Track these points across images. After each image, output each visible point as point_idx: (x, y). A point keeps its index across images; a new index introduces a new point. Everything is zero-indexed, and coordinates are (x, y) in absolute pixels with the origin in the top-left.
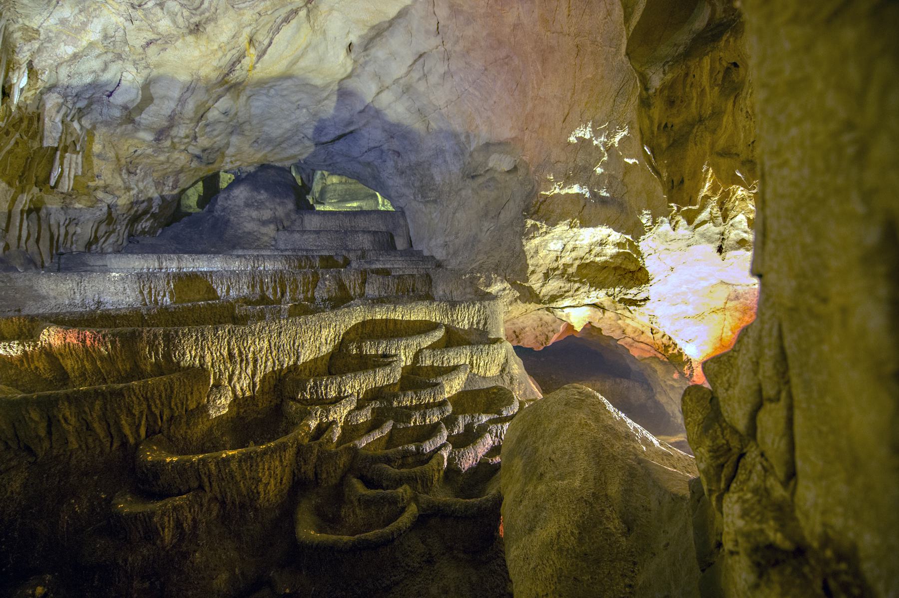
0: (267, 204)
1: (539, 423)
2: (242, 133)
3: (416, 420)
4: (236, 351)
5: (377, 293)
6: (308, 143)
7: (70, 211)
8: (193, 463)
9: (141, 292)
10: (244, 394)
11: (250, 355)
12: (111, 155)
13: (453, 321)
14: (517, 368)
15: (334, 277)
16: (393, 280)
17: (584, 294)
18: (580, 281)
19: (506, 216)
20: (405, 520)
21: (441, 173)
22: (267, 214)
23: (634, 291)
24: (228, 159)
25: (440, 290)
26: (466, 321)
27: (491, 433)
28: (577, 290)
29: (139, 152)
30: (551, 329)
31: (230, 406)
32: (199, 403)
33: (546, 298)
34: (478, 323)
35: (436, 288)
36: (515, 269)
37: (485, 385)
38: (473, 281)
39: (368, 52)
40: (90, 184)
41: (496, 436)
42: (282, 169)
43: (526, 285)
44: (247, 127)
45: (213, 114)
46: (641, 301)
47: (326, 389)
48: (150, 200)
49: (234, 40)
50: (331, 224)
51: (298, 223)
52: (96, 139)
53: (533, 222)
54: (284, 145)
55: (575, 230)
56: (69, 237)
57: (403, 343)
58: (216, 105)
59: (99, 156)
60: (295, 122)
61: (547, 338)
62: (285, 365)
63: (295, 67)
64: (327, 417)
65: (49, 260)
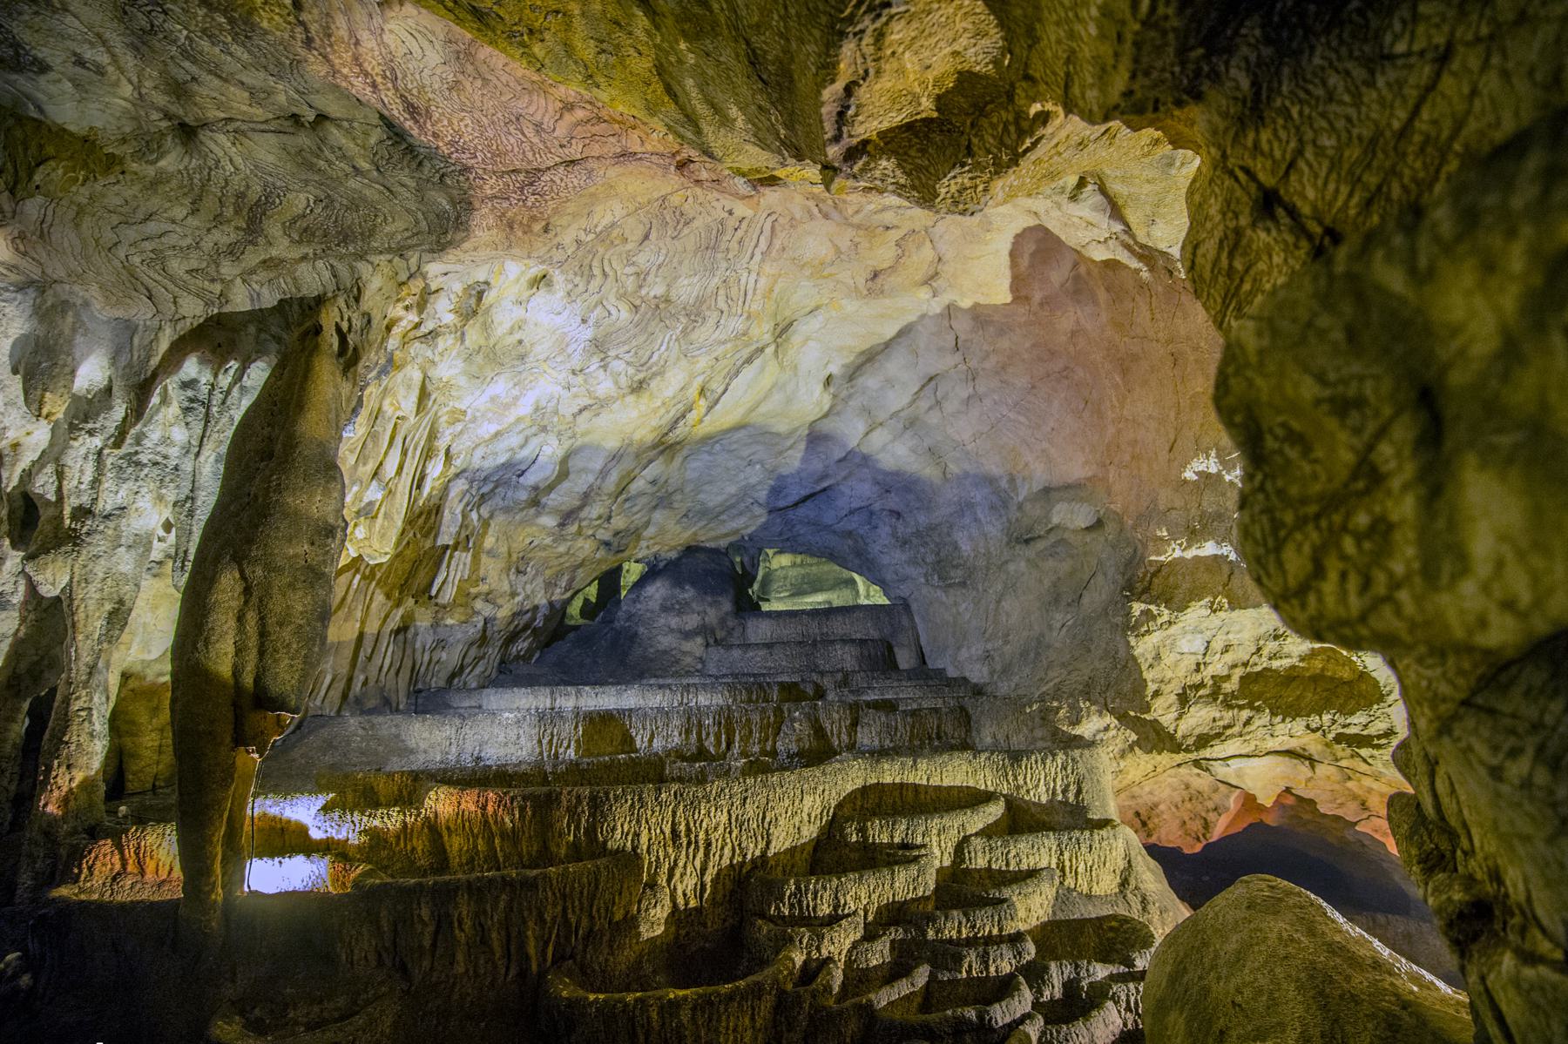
0: (694, 605)
1: (1205, 944)
2: (670, 506)
4: (682, 828)
5: (877, 743)
6: (758, 510)
10: (687, 904)
11: (702, 836)
13: (1018, 788)
14: (1151, 878)
15: (808, 716)
16: (903, 719)
17: (1262, 731)
18: (1251, 706)
19: (1094, 598)
21: (971, 538)
22: (692, 621)
23: (1359, 718)
24: (643, 544)
25: (986, 736)
26: (1042, 788)
28: (1248, 722)
30: (1210, 805)
33: (1190, 741)
34: (1064, 791)
35: (979, 732)
36: (1123, 691)
37: (1093, 912)
38: (1046, 716)
41: (1128, 1009)
42: (715, 551)
43: (1147, 717)
46: (1379, 737)
47: (815, 899)
50: (790, 631)
53: (1143, 606)
54: (723, 517)
55: (1222, 614)
57: (935, 823)
61: (1207, 825)
62: (749, 857)
64: (818, 949)
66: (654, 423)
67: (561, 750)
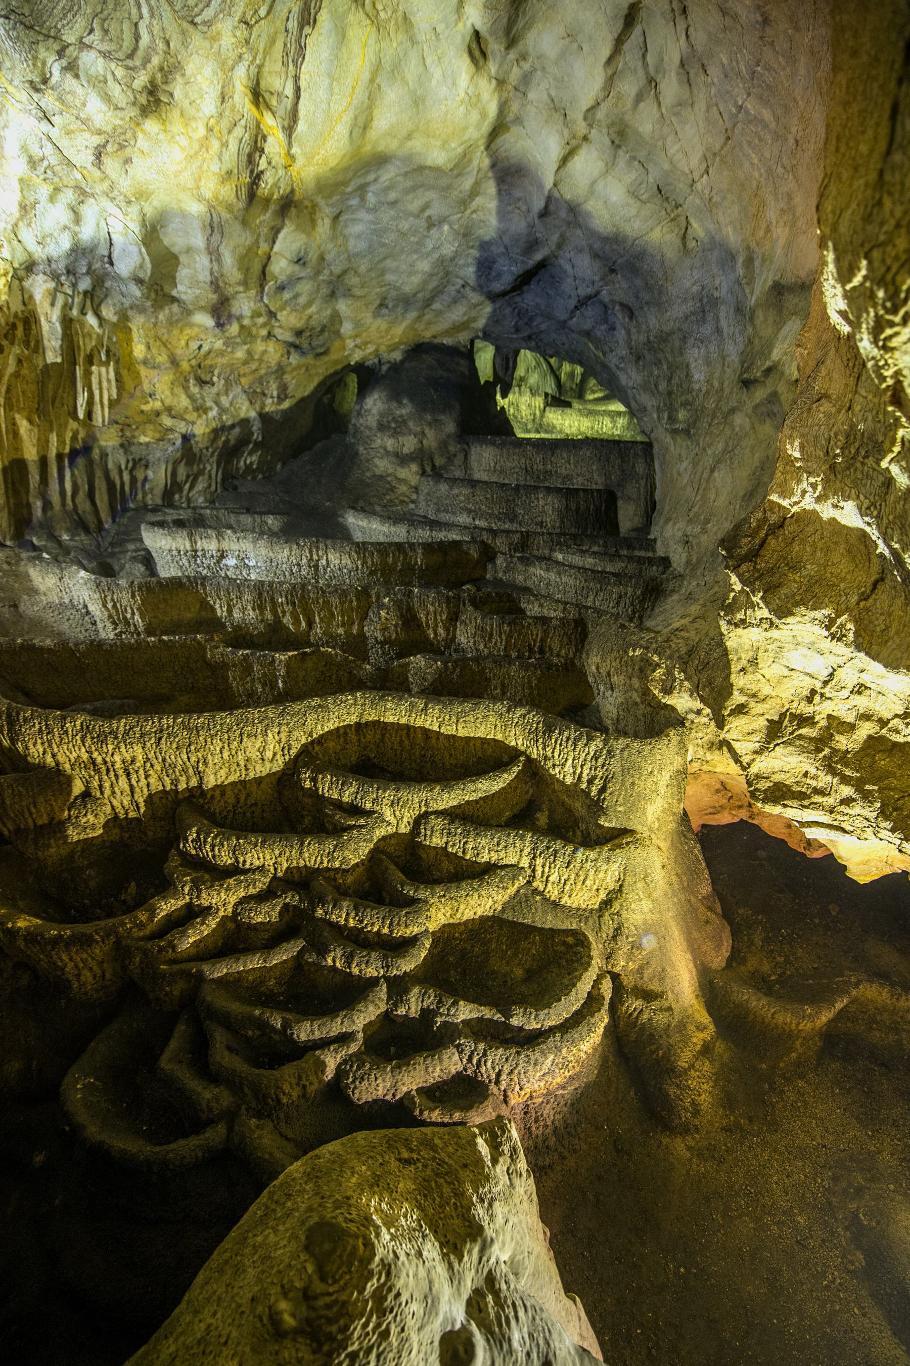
0: (411, 424)
2: (348, 293)
3: (334, 959)
6: (475, 297)
7: (133, 448)
9: (104, 606)
10: (127, 814)
11: (118, 765)
12: (162, 358)
15: (398, 604)
18: (859, 785)
21: (708, 362)
22: (409, 444)
24: (350, 344)
29: (206, 348)
31: (105, 826)
32: (53, 819)
34: (590, 782)
39: (520, 46)
40: (145, 408)
42: (452, 351)
44: (353, 280)
45: (280, 267)
47: (213, 850)
48: (245, 423)
49: (228, 105)
51: (458, 461)
52: (135, 335)
54: (436, 306)
56: (139, 485)
57: (388, 795)
58: (277, 248)
59: (145, 362)
60: (436, 255)
63: (373, 134)
65: (110, 520)
66: (215, 167)
67: (129, 616)
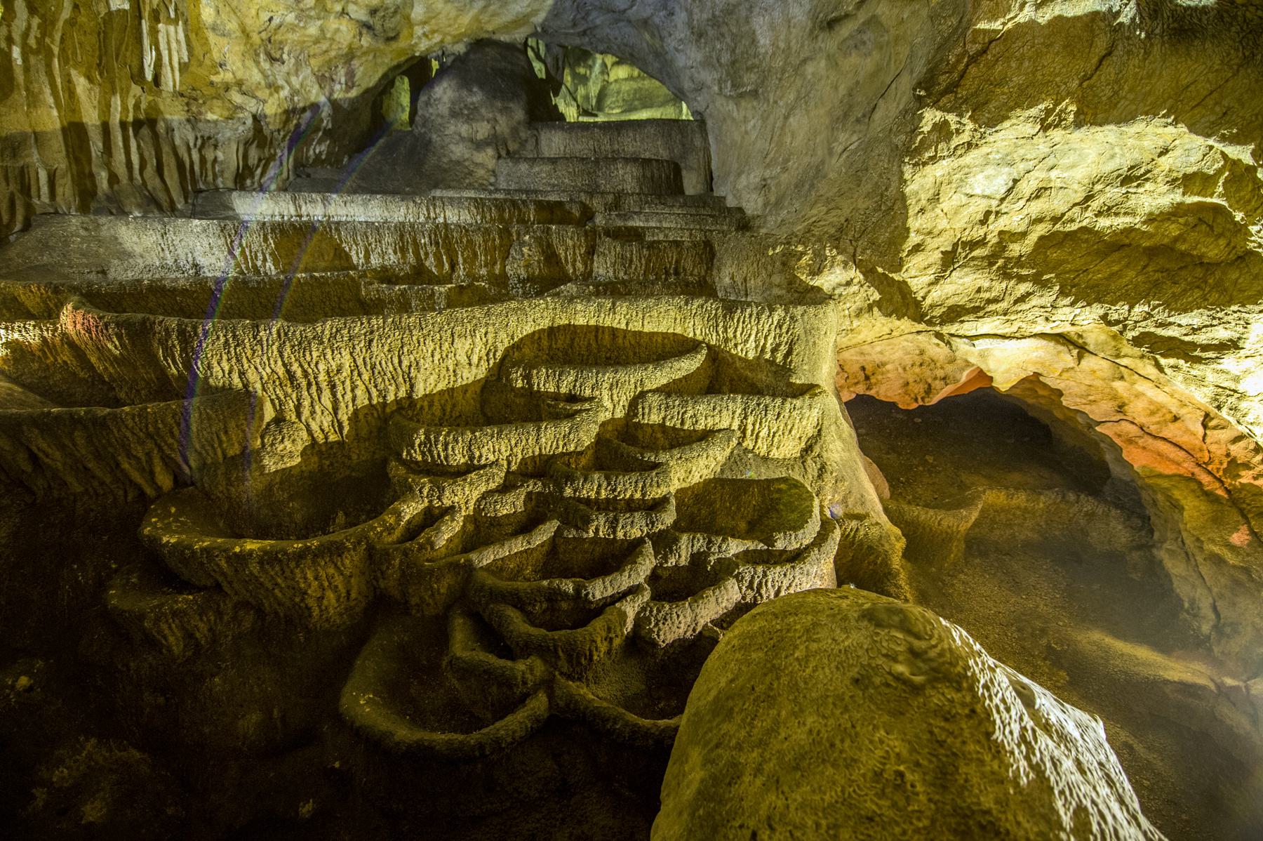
0: (483, 111)
3: (599, 527)
5: (611, 274)
7: (200, 125)
8: (194, 552)
9: (231, 253)
10: (326, 438)
12: (233, 26)
13: (727, 340)
14: (841, 447)
15: (539, 241)
16: (639, 251)
17: (1037, 312)
19: (887, 112)
20: (515, 723)
22: (483, 130)
23: (1195, 318)
24: (419, 31)
25: (725, 276)
26: (751, 344)
27: (739, 578)
28: (1022, 299)
29: (276, 21)
30: (940, 373)
31: (303, 453)
32: (246, 448)
33: (938, 312)
34: (774, 350)
35: (719, 270)
36: (876, 238)
37: (765, 474)
38: (788, 260)
40: (214, 78)
41: (750, 587)
42: (510, 47)
43: (896, 277)
46: (1205, 348)
47: (446, 449)
48: (315, 107)
50: (582, 146)
51: (530, 146)
53: (939, 114)
55: (1056, 134)
56: (209, 166)
57: (608, 377)
61: (929, 390)
62: (391, 398)
64: (439, 498)
65: (182, 200)
